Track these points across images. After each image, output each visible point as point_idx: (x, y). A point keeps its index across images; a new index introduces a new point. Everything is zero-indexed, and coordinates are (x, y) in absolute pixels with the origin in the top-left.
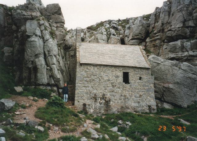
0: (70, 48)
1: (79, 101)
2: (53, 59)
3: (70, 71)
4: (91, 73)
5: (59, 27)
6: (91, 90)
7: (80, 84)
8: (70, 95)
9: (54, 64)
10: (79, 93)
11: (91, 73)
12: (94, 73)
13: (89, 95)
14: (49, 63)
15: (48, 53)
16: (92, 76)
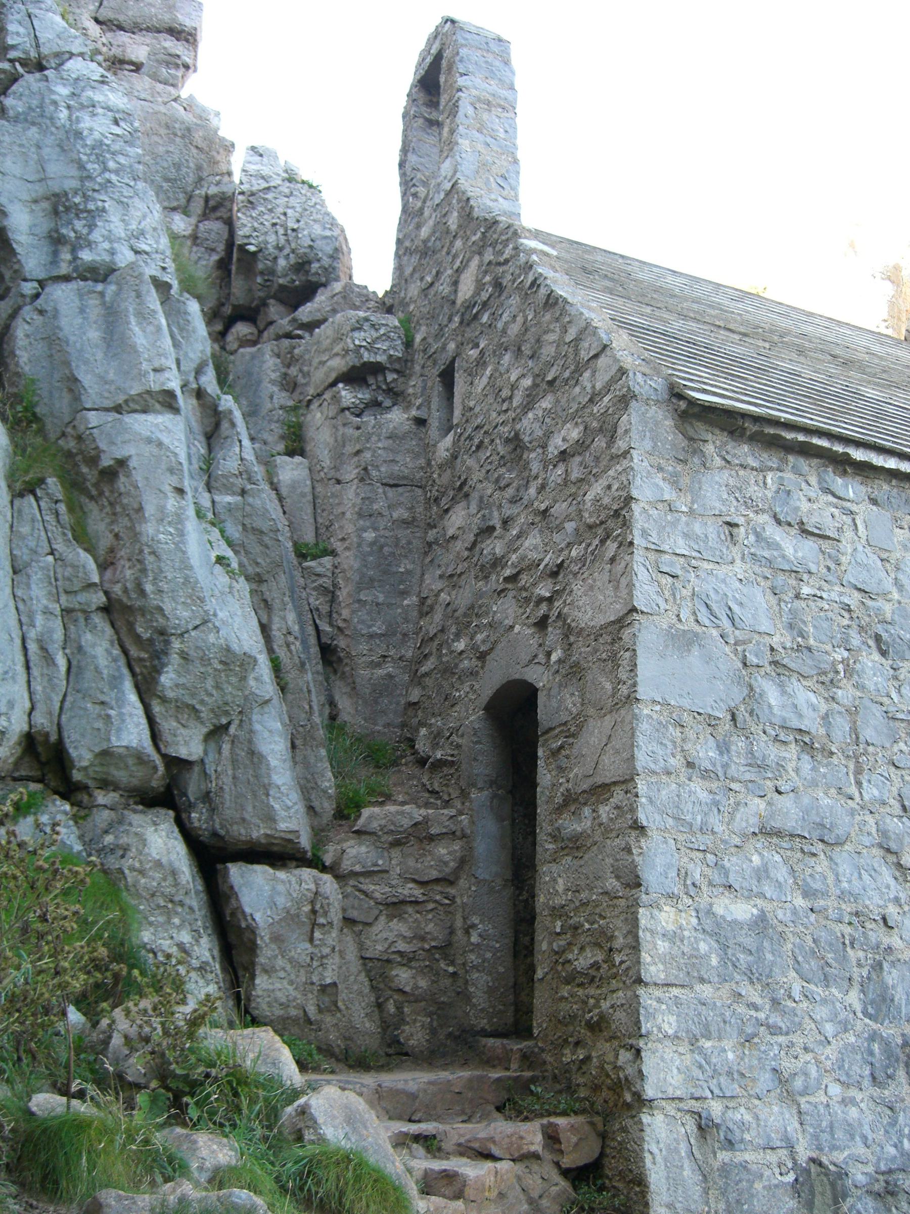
0: (308, 291)
1: (716, 1108)
2: (144, 316)
3: (331, 594)
4: (853, 599)
5: (137, 67)
6: (873, 903)
7: (699, 789)
8: (403, 976)
9: (168, 401)
10: (696, 957)
11: (853, 599)
12: (888, 609)
13: (854, 998)
14: (72, 383)
15: (56, 240)
16: (870, 660)
